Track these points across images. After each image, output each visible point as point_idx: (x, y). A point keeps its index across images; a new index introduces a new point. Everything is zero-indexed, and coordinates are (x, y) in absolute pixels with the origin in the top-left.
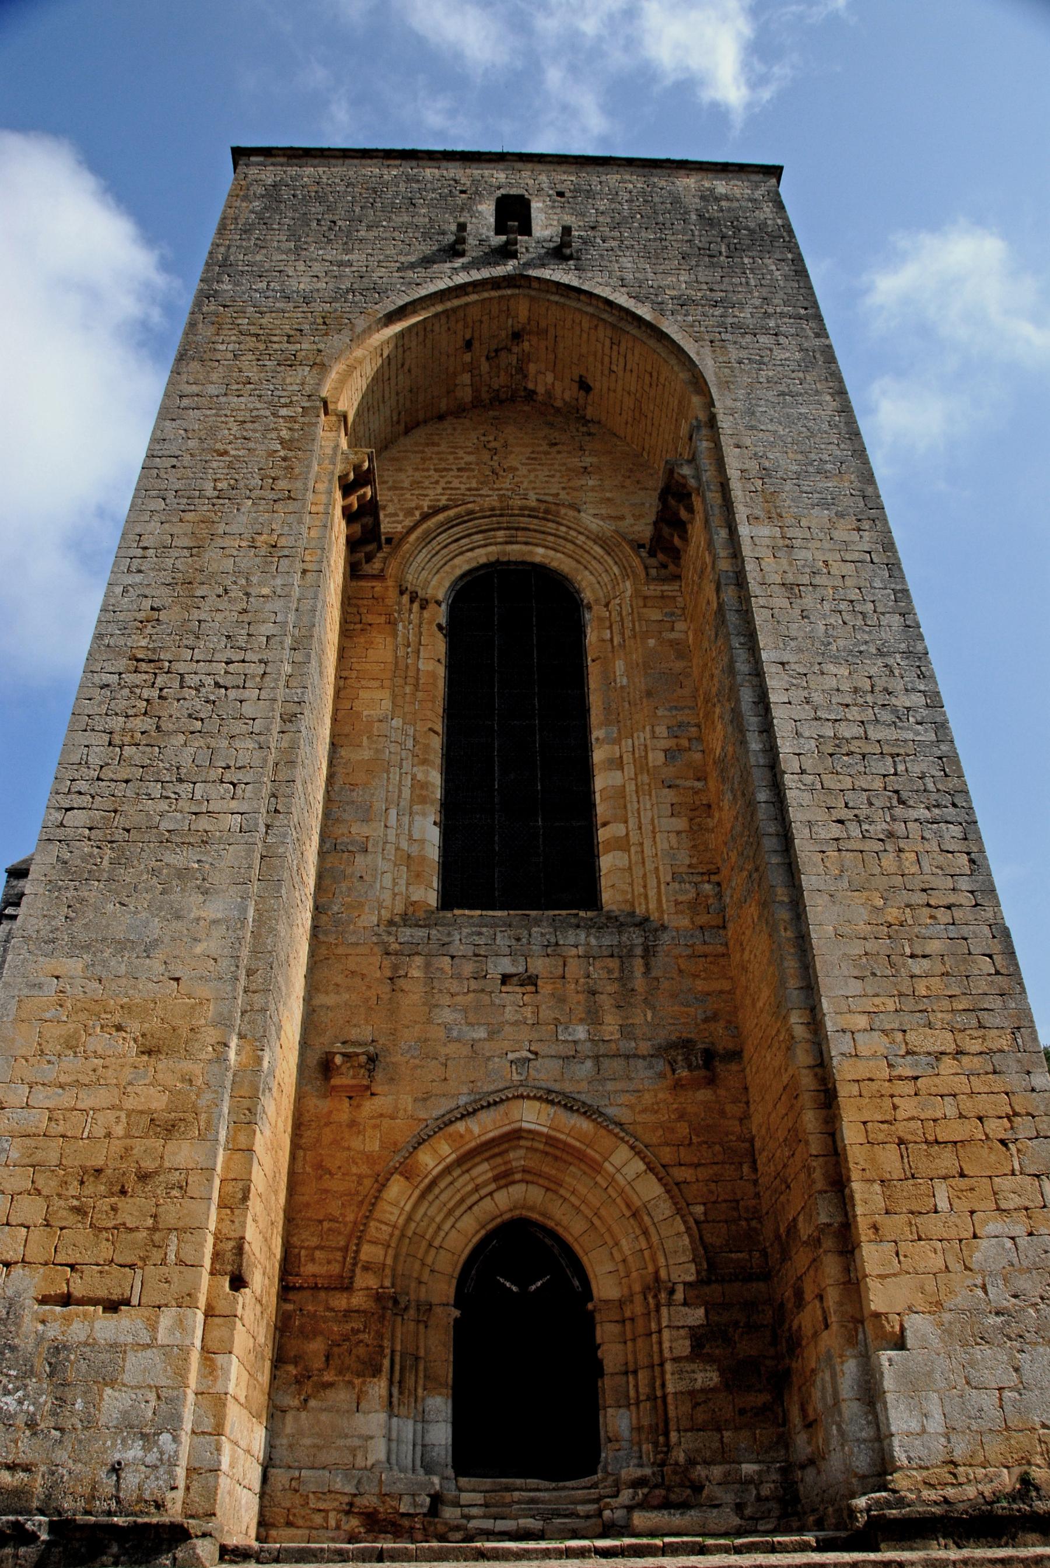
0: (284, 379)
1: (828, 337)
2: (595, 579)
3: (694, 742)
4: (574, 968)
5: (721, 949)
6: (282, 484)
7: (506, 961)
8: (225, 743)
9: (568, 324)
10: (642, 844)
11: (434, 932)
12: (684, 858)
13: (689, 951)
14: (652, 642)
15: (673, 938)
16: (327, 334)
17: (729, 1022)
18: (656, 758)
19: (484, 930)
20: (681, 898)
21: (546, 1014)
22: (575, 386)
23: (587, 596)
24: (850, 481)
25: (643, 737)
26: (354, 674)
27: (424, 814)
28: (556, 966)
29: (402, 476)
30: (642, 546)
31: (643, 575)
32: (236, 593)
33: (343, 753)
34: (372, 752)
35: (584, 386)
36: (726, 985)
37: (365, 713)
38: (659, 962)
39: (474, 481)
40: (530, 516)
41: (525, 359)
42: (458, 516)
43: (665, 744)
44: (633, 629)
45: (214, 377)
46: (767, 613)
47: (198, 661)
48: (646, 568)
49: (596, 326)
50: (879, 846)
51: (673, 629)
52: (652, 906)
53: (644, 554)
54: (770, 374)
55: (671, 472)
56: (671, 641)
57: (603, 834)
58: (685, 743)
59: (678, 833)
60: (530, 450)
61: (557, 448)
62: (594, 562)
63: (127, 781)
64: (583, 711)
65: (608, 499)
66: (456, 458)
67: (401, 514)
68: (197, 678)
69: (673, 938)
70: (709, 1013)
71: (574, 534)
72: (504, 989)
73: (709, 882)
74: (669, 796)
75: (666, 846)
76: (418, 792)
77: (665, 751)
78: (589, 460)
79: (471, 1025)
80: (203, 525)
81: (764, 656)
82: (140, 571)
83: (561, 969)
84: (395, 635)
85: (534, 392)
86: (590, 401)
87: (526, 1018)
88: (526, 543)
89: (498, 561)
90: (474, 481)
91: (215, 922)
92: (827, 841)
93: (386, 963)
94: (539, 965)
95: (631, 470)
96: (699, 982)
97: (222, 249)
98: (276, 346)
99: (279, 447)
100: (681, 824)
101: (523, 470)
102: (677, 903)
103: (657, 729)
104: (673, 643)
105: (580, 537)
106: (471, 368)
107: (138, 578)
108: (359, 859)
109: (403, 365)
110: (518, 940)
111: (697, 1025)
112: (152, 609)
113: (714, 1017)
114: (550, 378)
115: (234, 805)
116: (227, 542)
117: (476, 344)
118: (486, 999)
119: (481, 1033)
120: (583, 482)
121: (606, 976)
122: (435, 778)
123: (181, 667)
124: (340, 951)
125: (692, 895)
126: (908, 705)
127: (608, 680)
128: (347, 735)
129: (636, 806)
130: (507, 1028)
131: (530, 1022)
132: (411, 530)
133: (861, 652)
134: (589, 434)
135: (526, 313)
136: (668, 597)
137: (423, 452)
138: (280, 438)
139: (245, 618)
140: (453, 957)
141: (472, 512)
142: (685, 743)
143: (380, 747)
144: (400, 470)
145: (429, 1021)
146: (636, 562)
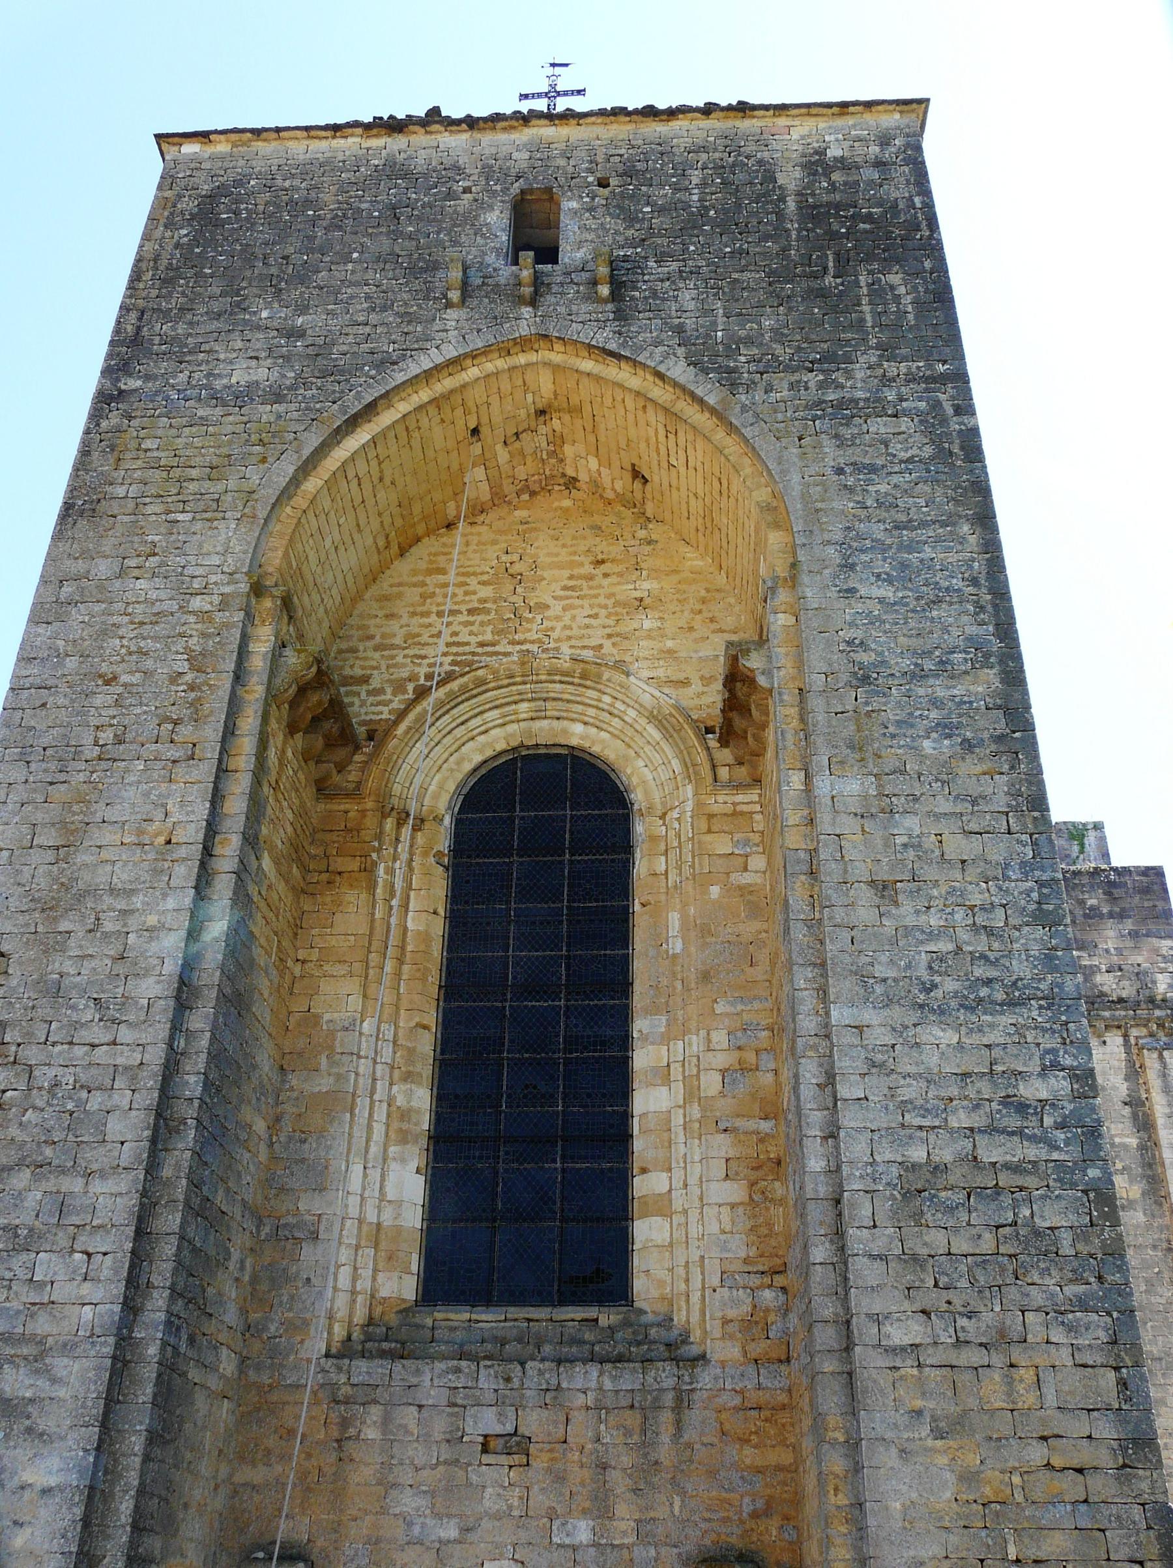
0: (200, 546)
1: (974, 414)
2: (651, 772)
3: (764, 1056)
4: (581, 1429)
5: (783, 1398)
6: (186, 732)
7: (490, 1414)
9: (608, 401)
10: (685, 1212)
11: (398, 1366)
12: (739, 1248)
13: (737, 1401)
14: (715, 891)
15: (716, 1378)
17: (787, 1518)
18: (711, 1083)
19: (464, 1363)
20: (731, 1313)
21: (540, 1500)
22: (628, 476)
23: (638, 797)
24: (985, 683)
25: (696, 1043)
26: (315, 955)
27: (403, 1161)
28: (555, 1422)
29: (394, 626)
30: (709, 730)
31: (709, 779)
33: (294, 1082)
34: (331, 1080)
36: (787, 1458)
37: (327, 1017)
38: (694, 1416)
39: (489, 629)
40: (561, 682)
41: (557, 441)
42: (464, 689)
43: (721, 1060)
44: (693, 866)
45: (107, 546)
46: (846, 935)
49: (644, 407)
50: (976, 1357)
51: (746, 869)
52: (695, 1318)
55: (735, 659)
56: (740, 888)
58: (751, 1057)
59: (733, 1206)
60: (566, 573)
61: (604, 568)
62: (647, 748)
64: (623, 985)
65: (670, 652)
66: (466, 593)
67: (389, 690)
69: (716, 1378)
70: (760, 1504)
71: (623, 707)
72: (486, 1459)
73: (770, 1286)
74: (722, 1145)
75: (714, 1228)
76: (395, 1125)
77: (723, 1072)
78: (646, 585)
79: (438, 1516)
81: (834, 1014)
83: (562, 1427)
84: (372, 887)
85: (575, 479)
86: (649, 495)
87: (510, 1507)
89: (522, 745)
90: (489, 629)
91: (46, 1491)
92: (903, 1349)
93: (334, 1417)
94: (533, 1422)
95: (703, 601)
96: (748, 1451)
97: (133, 315)
98: (192, 487)
100: (735, 1191)
101: (556, 608)
102: (726, 1322)
104: (743, 890)
106: (483, 461)
108: (307, 1250)
109: (381, 479)
110: (508, 1380)
111: (742, 1522)
113: (767, 1512)
114: (593, 463)
115: (86, 1289)
116: (109, 836)
117: (485, 431)
118: (461, 1473)
119: (450, 1531)
120: (635, 624)
121: (621, 1440)
122: (421, 1099)
124: (274, 1397)
125: (747, 1308)
127: (659, 941)
128: (300, 1054)
130: (486, 1524)
131: (516, 1513)
132: (402, 715)
135: (551, 386)
136: (742, 813)
137: (424, 584)
138: (188, 650)
139: (120, 969)
140: (420, 1406)
141: (484, 682)
142: (751, 1057)
143: (342, 1070)
144: (390, 616)
145: (383, 1511)
146: (701, 757)
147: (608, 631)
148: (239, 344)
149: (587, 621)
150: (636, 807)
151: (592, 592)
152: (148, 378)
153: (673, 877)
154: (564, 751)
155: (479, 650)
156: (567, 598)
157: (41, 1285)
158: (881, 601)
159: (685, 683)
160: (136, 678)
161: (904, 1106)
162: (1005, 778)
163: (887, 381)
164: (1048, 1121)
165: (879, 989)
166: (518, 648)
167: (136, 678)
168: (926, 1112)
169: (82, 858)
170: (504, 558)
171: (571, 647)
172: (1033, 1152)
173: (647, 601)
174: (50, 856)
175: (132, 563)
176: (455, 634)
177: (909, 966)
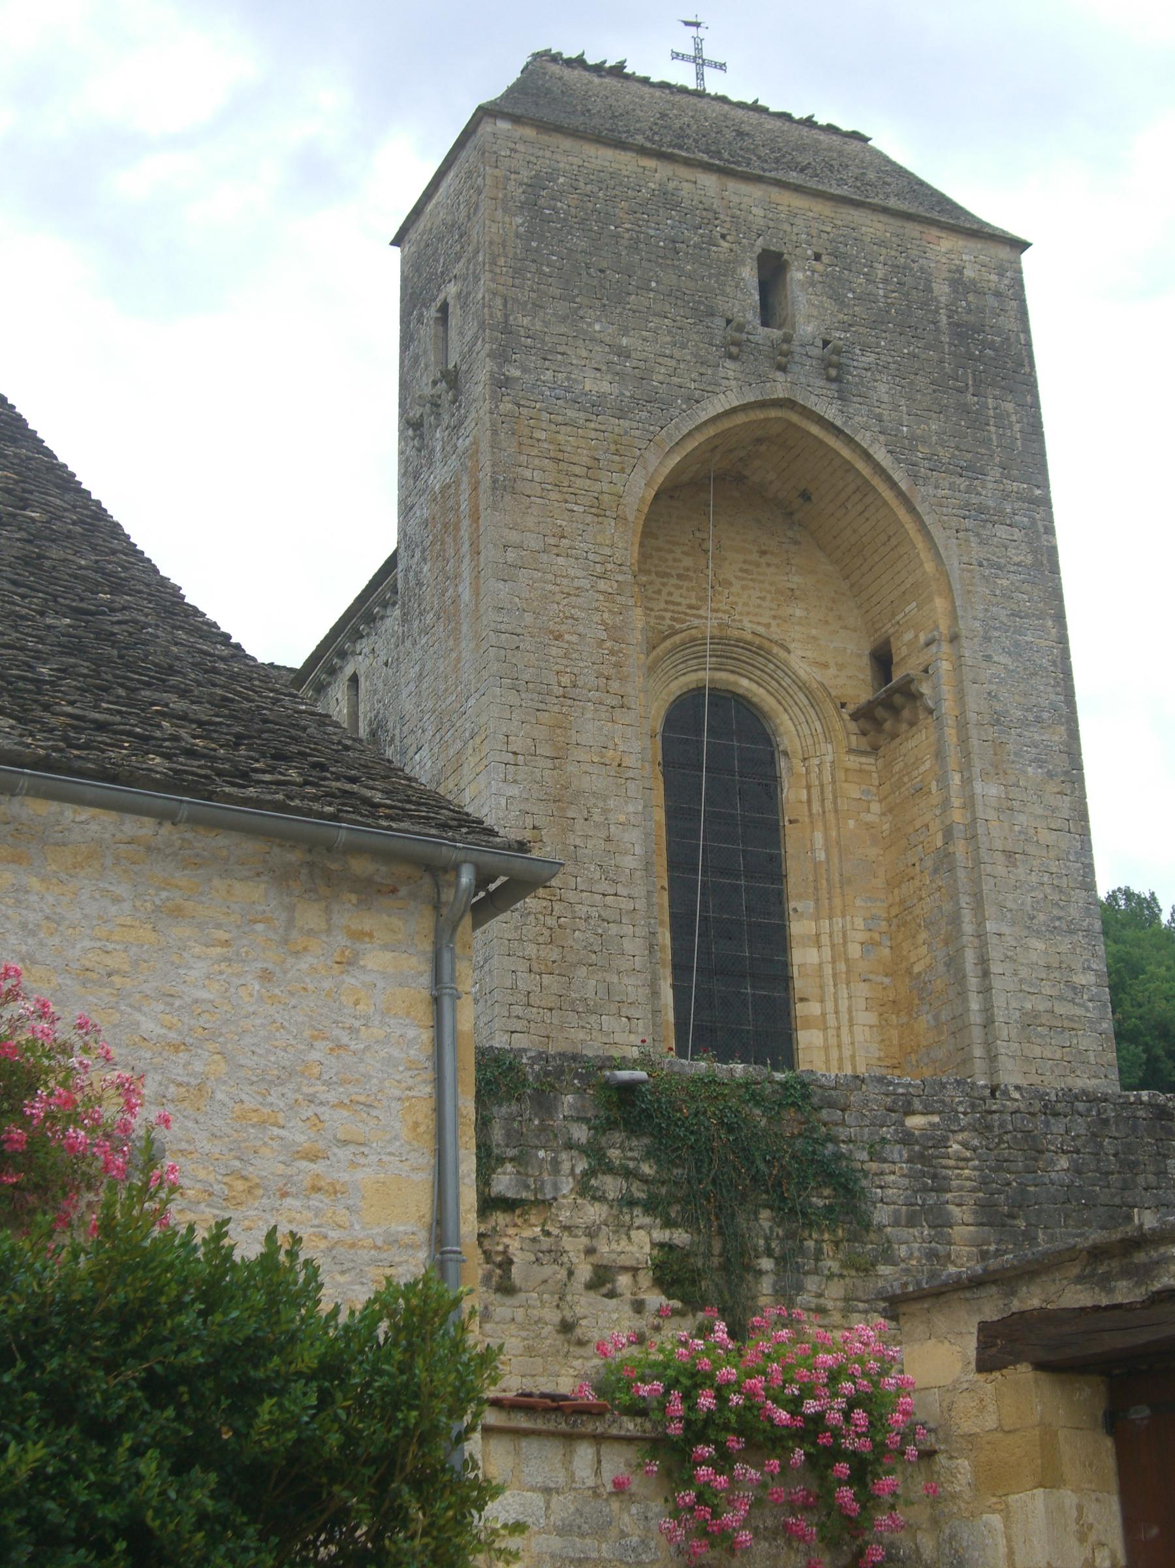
6: (615, 686)
8: (615, 979)
14: (851, 823)
16: (622, 471)
18: (855, 950)
32: (597, 818)
35: (806, 496)
43: (861, 936)
47: (582, 891)
48: (848, 734)
51: (869, 811)
53: (846, 717)
54: (1005, 583)
56: (867, 824)
57: (800, 1009)
58: (876, 936)
59: (871, 1027)
61: (768, 558)
62: (795, 708)
63: (551, 1009)
65: (814, 638)
66: (675, 560)
68: (585, 909)
74: (862, 990)
77: (862, 944)
78: (796, 579)
80: (558, 731)
82: (515, 781)
85: (746, 477)
88: (732, 672)
97: (499, 302)
98: (579, 483)
99: (604, 635)
100: (872, 1018)
103: (855, 919)
105: (787, 679)
107: (514, 791)
112: (534, 828)
114: (771, 476)
120: (790, 611)
123: (571, 896)
126: (1084, 983)
129: (832, 989)
133: (1055, 928)
134: (796, 543)
138: (603, 623)
142: (876, 936)
147: (773, 613)
148: (585, 354)
149: (759, 601)
150: (781, 748)
151: (761, 578)
152: (525, 370)
153: (816, 807)
154: (729, 695)
155: (688, 611)
156: (744, 579)
157: (607, 1034)
158: (1006, 667)
159: (825, 666)
160: (574, 638)
161: (1021, 981)
162: (1068, 798)
163: (1006, 496)
164: (1085, 997)
165: (1009, 915)
166: (715, 615)
167: (574, 638)
168: (1031, 985)
169: (571, 768)
170: (697, 534)
171: (750, 621)
172: (1079, 1012)
173: (797, 593)
174: (549, 764)
175: (552, 541)
176: (670, 594)
177: (1022, 904)
